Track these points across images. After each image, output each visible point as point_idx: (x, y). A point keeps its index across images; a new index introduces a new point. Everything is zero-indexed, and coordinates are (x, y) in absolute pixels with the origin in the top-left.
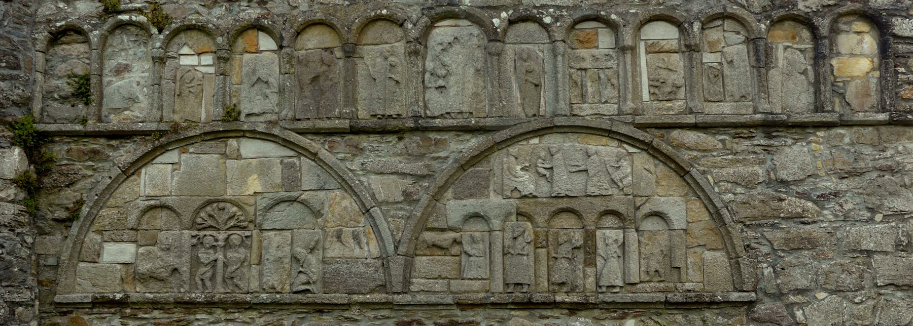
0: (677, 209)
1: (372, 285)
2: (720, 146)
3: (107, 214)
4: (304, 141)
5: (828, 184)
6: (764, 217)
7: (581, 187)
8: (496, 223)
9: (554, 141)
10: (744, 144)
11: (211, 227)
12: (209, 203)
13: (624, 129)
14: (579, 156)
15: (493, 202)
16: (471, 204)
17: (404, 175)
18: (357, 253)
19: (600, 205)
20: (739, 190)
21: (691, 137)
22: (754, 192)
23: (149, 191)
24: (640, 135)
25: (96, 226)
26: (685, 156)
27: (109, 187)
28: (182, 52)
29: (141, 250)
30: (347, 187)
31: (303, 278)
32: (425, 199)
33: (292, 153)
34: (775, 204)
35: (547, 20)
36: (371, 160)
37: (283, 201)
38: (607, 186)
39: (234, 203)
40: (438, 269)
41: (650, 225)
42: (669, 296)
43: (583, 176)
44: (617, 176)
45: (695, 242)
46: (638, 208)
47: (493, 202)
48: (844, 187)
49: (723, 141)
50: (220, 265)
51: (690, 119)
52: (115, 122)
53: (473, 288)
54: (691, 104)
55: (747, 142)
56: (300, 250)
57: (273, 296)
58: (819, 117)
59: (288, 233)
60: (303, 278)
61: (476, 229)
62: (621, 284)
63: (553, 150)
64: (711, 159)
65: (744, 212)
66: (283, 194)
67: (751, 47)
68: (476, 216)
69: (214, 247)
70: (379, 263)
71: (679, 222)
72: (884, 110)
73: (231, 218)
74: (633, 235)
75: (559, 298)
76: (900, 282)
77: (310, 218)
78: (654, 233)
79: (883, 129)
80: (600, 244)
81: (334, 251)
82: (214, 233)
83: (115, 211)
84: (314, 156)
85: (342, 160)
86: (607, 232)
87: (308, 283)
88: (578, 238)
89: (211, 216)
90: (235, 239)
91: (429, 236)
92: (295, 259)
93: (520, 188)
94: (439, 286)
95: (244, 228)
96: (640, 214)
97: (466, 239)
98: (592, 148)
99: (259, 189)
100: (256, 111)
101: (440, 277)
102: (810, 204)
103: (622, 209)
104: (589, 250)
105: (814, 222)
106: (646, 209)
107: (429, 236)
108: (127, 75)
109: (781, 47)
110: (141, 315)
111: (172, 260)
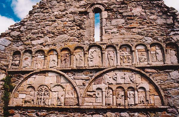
1: (75, 104)
3: (20, 88)
6: (169, 88)
7: (124, 81)
8: (104, 90)
9: (117, 72)
11: (41, 91)
12: (41, 86)
13: (133, 68)
14: (123, 75)
15: (103, 86)
18: (72, 97)
19: (128, 86)
24: (137, 69)
25: (18, 90)
27: (21, 82)
28: (38, 55)
29: (27, 96)
30: (70, 82)
31: (60, 102)
32: (87, 85)
33: (59, 75)
36: (76, 77)
37: (56, 85)
38: (130, 81)
39: (46, 86)
41: (140, 90)
42: (146, 107)
43: (124, 79)
44: (132, 79)
45: (152, 94)
46: (137, 86)
47: (103, 86)
50: (42, 99)
51: (149, 66)
52: (24, 69)
54: (149, 62)
56: (60, 96)
57: (53, 106)
59: (57, 92)
60: (60, 102)
62: (134, 104)
63: (117, 74)
64: (155, 75)
65: (163, 87)
66: (56, 84)
68: (98, 89)
69: (41, 95)
70: (77, 99)
71: (147, 89)
73: (45, 89)
74: (136, 92)
77: (63, 90)
78: (142, 92)
80: (128, 95)
81: (67, 96)
82: (41, 92)
84: (64, 76)
85: (70, 76)
86: (130, 92)
87: (61, 103)
88: (123, 93)
89: (41, 88)
90: (46, 94)
91: (89, 93)
92: (58, 98)
93: (109, 82)
95: (48, 91)
96: (138, 88)
100: (52, 66)
101: (91, 102)
103: (133, 87)
104: (126, 96)
106: (139, 87)
107: (89, 93)
108: (27, 60)
111: (32, 97)
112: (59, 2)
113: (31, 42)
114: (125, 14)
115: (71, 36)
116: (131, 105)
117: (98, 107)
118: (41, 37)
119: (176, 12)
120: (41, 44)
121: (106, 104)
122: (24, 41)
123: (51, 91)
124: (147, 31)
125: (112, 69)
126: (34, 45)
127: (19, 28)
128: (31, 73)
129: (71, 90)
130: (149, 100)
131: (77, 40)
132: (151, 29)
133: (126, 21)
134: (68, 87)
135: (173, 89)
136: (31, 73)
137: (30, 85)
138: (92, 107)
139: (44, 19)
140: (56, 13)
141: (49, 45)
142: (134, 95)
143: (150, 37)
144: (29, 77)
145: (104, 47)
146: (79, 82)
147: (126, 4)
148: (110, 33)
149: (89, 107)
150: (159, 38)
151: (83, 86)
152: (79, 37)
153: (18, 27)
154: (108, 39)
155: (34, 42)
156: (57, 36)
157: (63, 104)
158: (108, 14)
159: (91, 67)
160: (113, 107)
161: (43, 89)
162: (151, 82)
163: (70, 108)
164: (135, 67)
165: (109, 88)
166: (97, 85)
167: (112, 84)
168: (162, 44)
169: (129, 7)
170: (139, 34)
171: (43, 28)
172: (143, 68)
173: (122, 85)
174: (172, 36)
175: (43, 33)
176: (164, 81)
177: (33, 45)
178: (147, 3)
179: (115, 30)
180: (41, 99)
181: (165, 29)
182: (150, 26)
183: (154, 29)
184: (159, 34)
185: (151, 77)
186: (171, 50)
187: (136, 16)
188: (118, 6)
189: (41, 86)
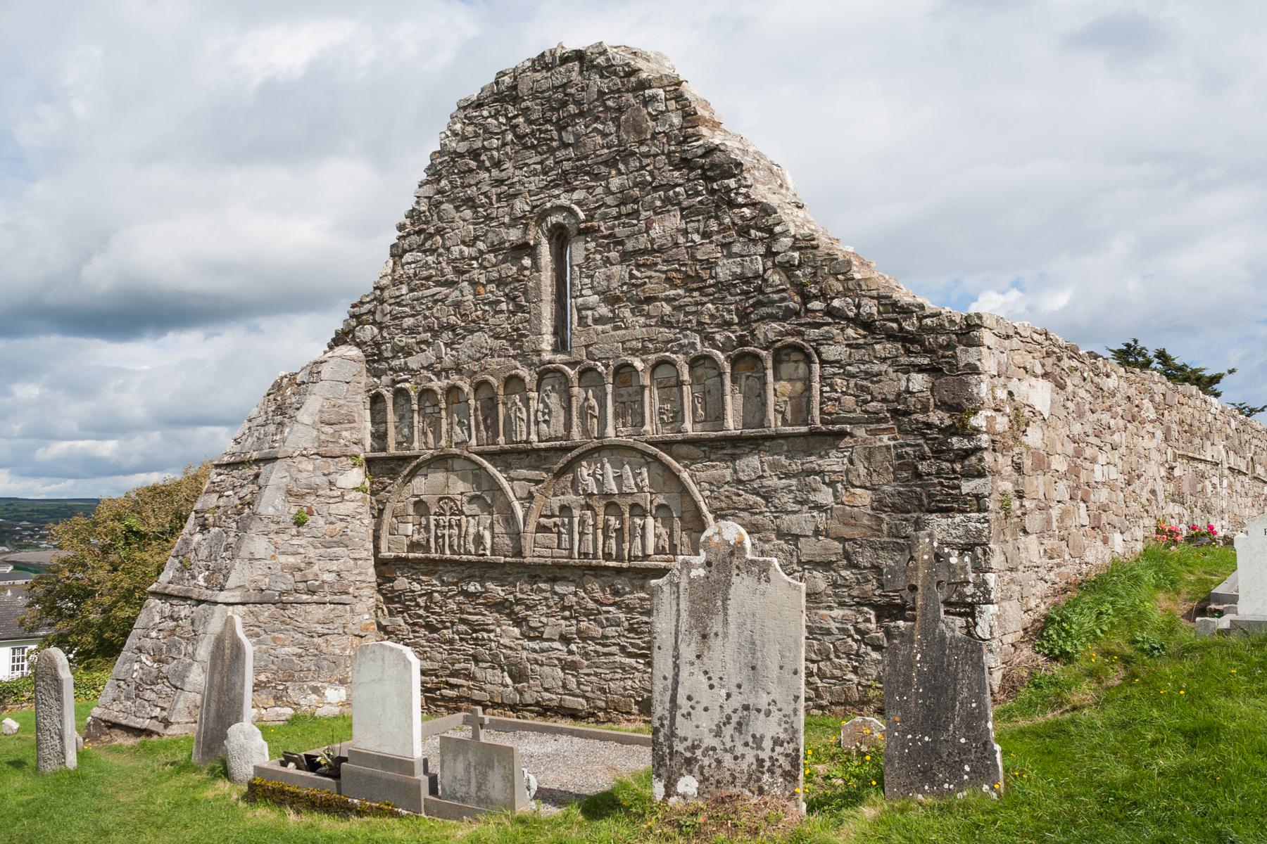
0: (675, 502)
2: (703, 455)
5: (773, 482)
6: (729, 509)
11: (441, 514)
12: (441, 499)
13: (640, 446)
17: (529, 481)
21: (684, 450)
22: (722, 490)
23: (415, 493)
38: (633, 486)
49: (704, 451)
51: (680, 437)
72: (807, 425)
74: (650, 520)
76: (818, 559)
79: (810, 439)
83: (402, 504)
91: (543, 520)
94: (547, 552)
99: (463, 490)
102: (759, 499)
103: (642, 503)
105: (761, 513)
107: (543, 520)
109: (744, 376)
110: (415, 566)
112: (461, 206)
113: (406, 363)
114: (630, 245)
115: (496, 338)
116: (636, 558)
117: (562, 560)
118: (425, 342)
119: (778, 224)
120: (429, 367)
121: (580, 554)
122: (388, 358)
123: (461, 513)
124: (687, 309)
125: (593, 449)
126: (413, 370)
127: (372, 313)
128: (414, 463)
130: (679, 546)
131: (512, 352)
132: (697, 304)
133: (632, 276)
135: (742, 514)
136: (414, 463)
137: (417, 496)
138: (549, 561)
139: (428, 278)
140: (455, 251)
141: (446, 370)
142: (643, 528)
143: (695, 331)
144: (412, 474)
145: (572, 373)
147: (636, 201)
148: (590, 321)
149: (542, 560)
150: (718, 337)
152: (516, 340)
153: (370, 311)
154: (587, 347)
155: (414, 362)
156: (464, 338)
157: (488, 552)
158: (587, 249)
159: (547, 441)
160: (594, 562)
161: (445, 507)
163: (505, 563)
164: (646, 442)
165: (589, 507)
166: (562, 497)
167: (592, 494)
169: (644, 214)
170: (664, 322)
171: (427, 313)
172: (666, 445)
173: (616, 499)
174: (754, 325)
175: (429, 329)
176: (718, 488)
177: (413, 373)
178: (698, 194)
179: (604, 310)
180: (444, 535)
181: (738, 298)
182: (695, 290)
183: (705, 299)
184: (719, 321)
185: (685, 475)
186: (748, 377)
187: (660, 250)
188: (614, 211)
189: (441, 499)
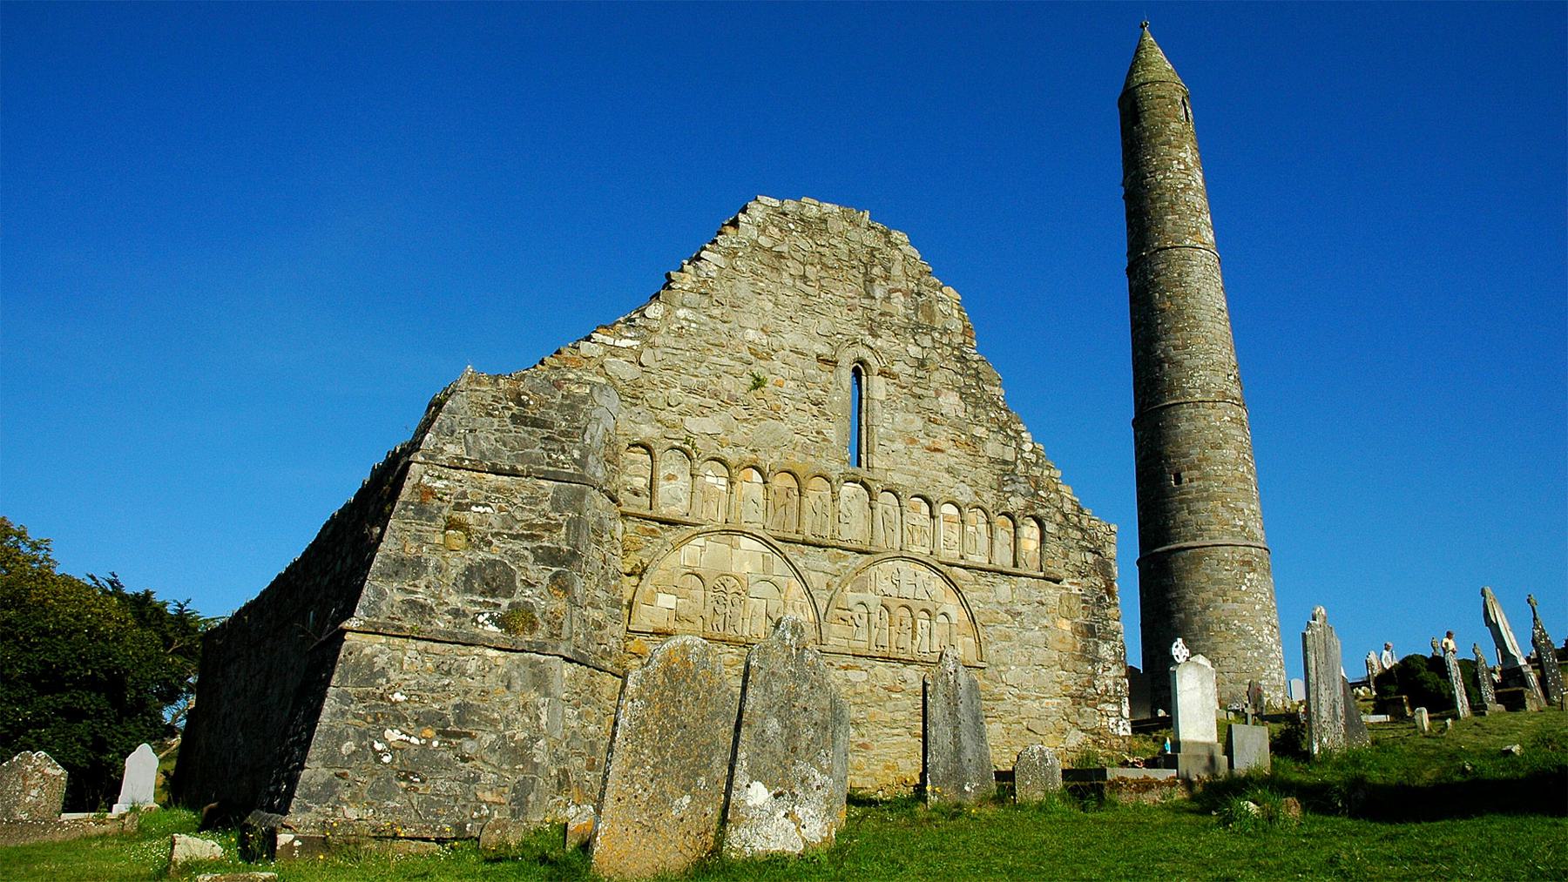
4: (778, 544)
5: (1019, 608)
6: (991, 622)
9: (899, 563)
10: (982, 580)
15: (872, 599)
16: (861, 596)
19: (921, 605)
20: (981, 605)
26: (959, 583)
34: (996, 615)
35: (900, 493)
40: (844, 633)
46: (937, 609)
48: (1023, 610)
53: (862, 647)
55: (984, 579)
58: (1016, 571)
59: (764, 601)
61: (862, 609)
66: (762, 577)
67: (989, 526)
75: (902, 656)
78: (943, 624)
96: (938, 613)
97: (856, 617)
98: (918, 572)
129: (800, 599)
134: (796, 587)
146: (816, 579)
151: (826, 592)
162: (964, 603)
168: (990, 511)
